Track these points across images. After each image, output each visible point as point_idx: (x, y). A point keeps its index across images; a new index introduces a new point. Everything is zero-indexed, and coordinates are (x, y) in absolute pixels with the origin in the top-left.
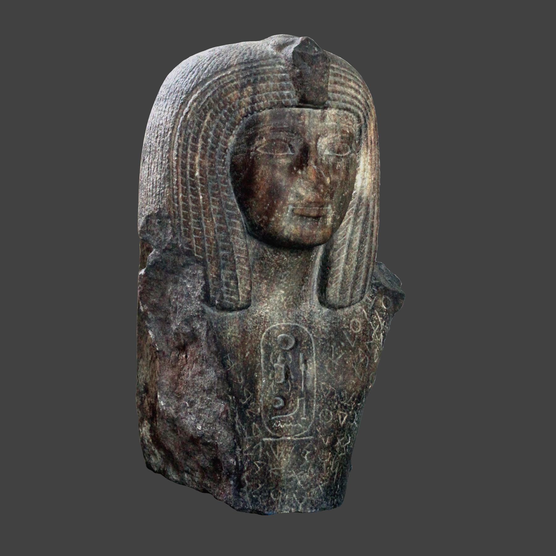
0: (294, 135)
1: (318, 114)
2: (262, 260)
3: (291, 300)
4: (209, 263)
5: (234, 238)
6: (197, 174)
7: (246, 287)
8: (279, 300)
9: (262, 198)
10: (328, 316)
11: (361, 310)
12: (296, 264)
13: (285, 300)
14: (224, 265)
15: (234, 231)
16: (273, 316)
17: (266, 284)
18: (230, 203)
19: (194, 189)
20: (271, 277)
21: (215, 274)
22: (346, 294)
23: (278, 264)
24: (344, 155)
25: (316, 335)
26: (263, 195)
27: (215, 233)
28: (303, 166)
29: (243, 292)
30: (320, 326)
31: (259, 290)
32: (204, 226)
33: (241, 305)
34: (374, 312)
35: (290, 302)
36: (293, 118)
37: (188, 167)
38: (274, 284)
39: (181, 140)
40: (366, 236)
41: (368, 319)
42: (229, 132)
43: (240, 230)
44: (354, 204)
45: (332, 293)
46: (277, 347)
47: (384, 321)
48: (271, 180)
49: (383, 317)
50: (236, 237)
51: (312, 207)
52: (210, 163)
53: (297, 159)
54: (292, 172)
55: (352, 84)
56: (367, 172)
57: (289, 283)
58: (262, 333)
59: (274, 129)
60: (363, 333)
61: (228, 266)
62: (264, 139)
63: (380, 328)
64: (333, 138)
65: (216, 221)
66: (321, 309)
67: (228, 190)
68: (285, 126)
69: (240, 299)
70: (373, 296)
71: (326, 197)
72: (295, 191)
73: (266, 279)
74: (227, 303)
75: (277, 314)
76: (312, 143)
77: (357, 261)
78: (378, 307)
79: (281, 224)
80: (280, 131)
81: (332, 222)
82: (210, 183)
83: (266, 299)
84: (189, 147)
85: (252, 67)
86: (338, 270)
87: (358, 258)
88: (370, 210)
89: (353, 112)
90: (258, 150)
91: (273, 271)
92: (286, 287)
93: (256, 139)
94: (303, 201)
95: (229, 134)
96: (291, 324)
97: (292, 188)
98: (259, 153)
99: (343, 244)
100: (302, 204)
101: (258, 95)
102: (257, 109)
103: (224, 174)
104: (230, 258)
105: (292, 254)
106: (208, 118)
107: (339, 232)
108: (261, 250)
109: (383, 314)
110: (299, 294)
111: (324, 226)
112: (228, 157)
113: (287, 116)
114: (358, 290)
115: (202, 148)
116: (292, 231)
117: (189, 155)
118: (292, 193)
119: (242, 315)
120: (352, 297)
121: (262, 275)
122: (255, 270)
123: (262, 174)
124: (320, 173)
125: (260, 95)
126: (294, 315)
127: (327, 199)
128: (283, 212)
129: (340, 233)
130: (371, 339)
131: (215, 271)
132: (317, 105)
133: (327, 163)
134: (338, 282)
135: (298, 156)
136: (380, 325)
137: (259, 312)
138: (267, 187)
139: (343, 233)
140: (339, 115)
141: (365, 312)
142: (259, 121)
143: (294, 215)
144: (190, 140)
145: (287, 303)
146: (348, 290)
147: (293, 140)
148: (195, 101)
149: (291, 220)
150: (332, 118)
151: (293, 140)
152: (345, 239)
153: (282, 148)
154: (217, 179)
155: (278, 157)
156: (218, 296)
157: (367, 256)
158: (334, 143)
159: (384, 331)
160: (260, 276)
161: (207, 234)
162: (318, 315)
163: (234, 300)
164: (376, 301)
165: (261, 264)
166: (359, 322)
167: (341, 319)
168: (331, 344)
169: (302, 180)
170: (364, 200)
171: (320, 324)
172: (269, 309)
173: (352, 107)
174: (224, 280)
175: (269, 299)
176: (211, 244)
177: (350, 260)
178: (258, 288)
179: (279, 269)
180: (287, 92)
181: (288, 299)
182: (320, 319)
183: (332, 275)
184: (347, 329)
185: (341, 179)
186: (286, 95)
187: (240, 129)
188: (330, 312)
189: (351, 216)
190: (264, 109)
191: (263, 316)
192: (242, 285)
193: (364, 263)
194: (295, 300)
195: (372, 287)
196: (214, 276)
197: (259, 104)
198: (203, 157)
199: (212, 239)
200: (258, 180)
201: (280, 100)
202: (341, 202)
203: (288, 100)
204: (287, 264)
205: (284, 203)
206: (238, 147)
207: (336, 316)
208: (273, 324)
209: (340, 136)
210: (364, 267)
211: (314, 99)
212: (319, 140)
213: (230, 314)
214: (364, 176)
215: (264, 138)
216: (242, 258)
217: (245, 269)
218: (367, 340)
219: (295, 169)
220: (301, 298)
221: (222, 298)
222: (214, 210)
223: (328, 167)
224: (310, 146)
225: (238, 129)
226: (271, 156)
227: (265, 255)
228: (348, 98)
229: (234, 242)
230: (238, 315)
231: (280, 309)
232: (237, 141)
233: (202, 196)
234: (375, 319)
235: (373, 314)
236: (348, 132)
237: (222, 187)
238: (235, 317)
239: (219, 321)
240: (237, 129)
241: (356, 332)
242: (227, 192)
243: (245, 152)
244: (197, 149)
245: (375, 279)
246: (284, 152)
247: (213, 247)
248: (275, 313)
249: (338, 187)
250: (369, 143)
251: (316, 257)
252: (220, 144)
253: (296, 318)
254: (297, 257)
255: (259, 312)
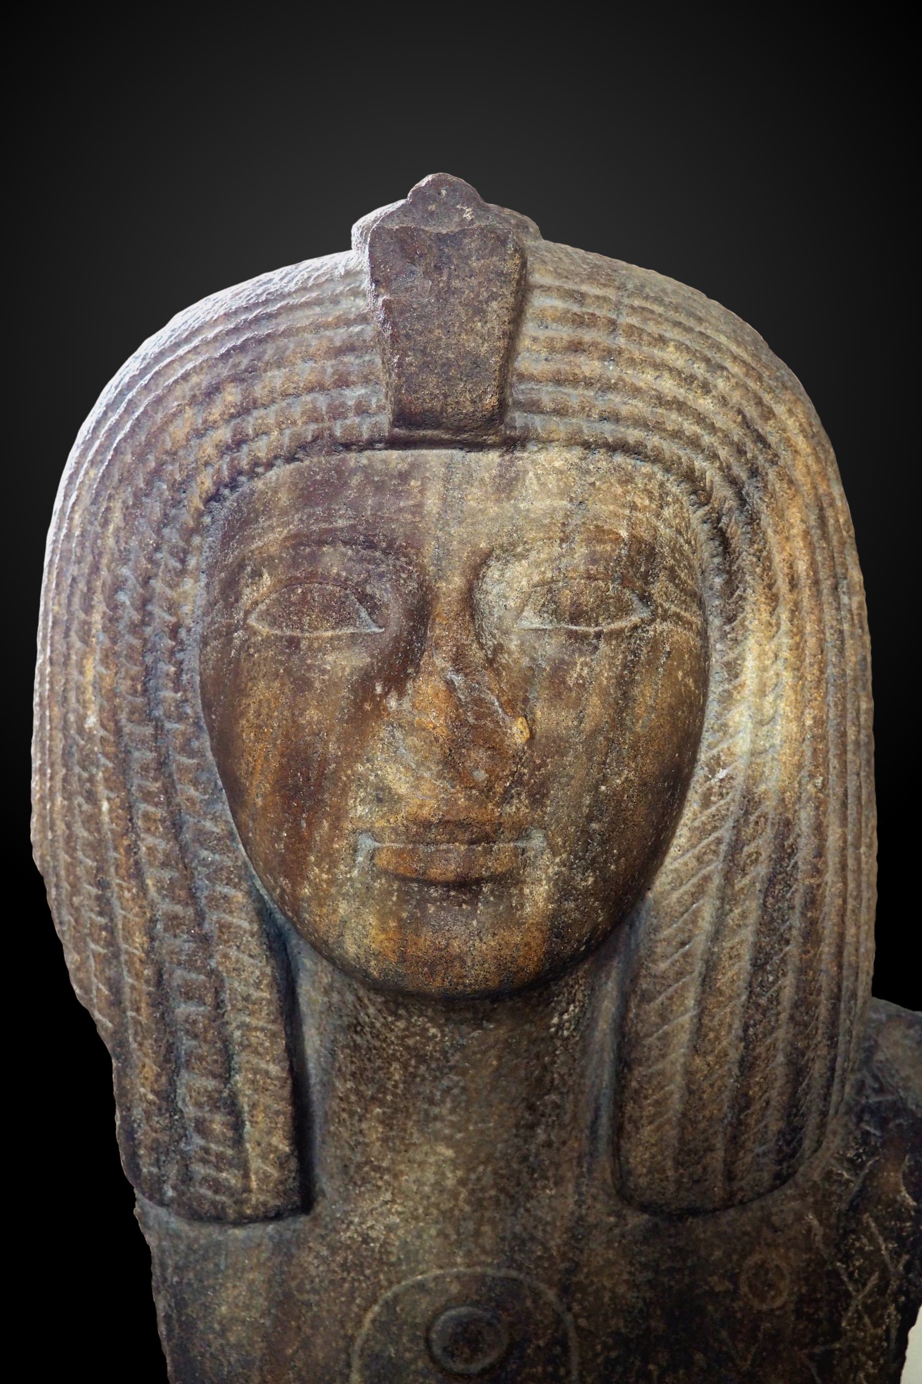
0: (378, 554)
1: (488, 468)
2: (356, 1032)
3: (488, 1180)
4: (134, 1046)
5: (226, 956)
6: (92, 721)
7: (275, 1141)
8: (437, 1183)
9: (264, 808)
10: (645, 1241)
11: (799, 1218)
12: (484, 1053)
13: (462, 1182)
14: (189, 1054)
15: (223, 927)
16: (418, 1243)
17: (382, 1122)
18: (208, 825)
19: (85, 775)
20: (395, 1095)
21: (153, 1091)
22: (705, 1169)
23: (407, 1048)
24: (606, 628)
25: (587, 1318)
26: (264, 796)
27: (152, 939)
28: (408, 676)
29: (264, 1157)
30: (608, 1284)
31: (358, 1143)
32: (120, 912)
33: (255, 1208)
34: (859, 1222)
35: (483, 1190)
36: (380, 488)
37: (72, 699)
38: (410, 1124)
39: (60, 605)
40: (788, 942)
41: (825, 1253)
42: (178, 565)
43: (246, 925)
44: (724, 818)
45: (642, 1162)
46: (420, 1364)
47: (906, 1257)
48: (287, 736)
49: (900, 1240)
50: (233, 953)
51: (435, 842)
52: (129, 683)
53: (393, 652)
54: (364, 700)
55: (670, 355)
56: (779, 697)
57: (468, 1120)
58: (366, 1310)
59: (295, 536)
60: (799, 1314)
61: (201, 1058)
62: (267, 579)
63: (887, 1284)
64: (551, 560)
65: (159, 890)
66: (619, 1215)
67: (204, 778)
68: (341, 523)
69: (254, 1185)
70: (859, 1155)
71: (506, 798)
72: (372, 778)
73: (382, 1103)
74: (203, 1197)
75: (433, 1232)
76: (448, 582)
77: (745, 1038)
78: (879, 1201)
79: (335, 911)
80: (321, 543)
81: (549, 899)
82: (136, 754)
83: (386, 1177)
84: (75, 626)
85: (257, 320)
86: (661, 1073)
87: (746, 1028)
88: (802, 841)
89: (656, 458)
90: (252, 621)
91: (397, 1077)
92: (459, 1136)
93: (243, 582)
94: (399, 819)
95: (175, 569)
96: (490, 1271)
97: (360, 768)
98: (255, 633)
99: (680, 974)
100: (394, 830)
101: (255, 413)
102: (244, 464)
103: (181, 718)
104: (206, 1031)
105: (454, 1016)
106: (117, 517)
107: (656, 929)
108: (350, 998)
109: (902, 1229)
110: (525, 1158)
111: (510, 918)
112: (191, 658)
113: (355, 481)
114: (759, 1150)
115: (105, 629)
116: (366, 941)
117: (74, 657)
118: (360, 786)
119: (288, 1235)
120: (730, 1176)
121: (362, 1088)
122: (340, 1070)
123: (258, 714)
124: (479, 702)
125: (262, 412)
126: (508, 1235)
127: (517, 808)
128: (334, 864)
129: (666, 933)
130: (837, 1333)
131: (152, 1079)
132: (459, 430)
133: (525, 662)
134: (669, 1121)
135: (397, 640)
136: (884, 1270)
137: (361, 1223)
138: (274, 764)
139: (681, 930)
140: (588, 472)
141: (815, 1223)
142: (256, 511)
143: (378, 877)
144: (76, 600)
145: (471, 1193)
146: (711, 1149)
147: (381, 575)
148: (92, 463)
149: (365, 895)
150: (552, 482)
151: (381, 575)
152: (686, 955)
153: (326, 609)
154: (155, 737)
155: (316, 645)
156: (173, 1171)
157: (792, 1018)
158: (553, 581)
159: (907, 1294)
160: (357, 1092)
161: (126, 939)
162: (604, 1238)
163: (229, 1188)
164: (871, 1175)
165: (356, 1047)
166: (783, 1265)
167: (703, 1253)
168: (645, 1361)
169: (398, 734)
170: (769, 806)
171: (611, 1276)
172: (399, 1213)
173: (654, 441)
174: (191, 1111)
175: (396, 1176)
176: (138, 976)
177: (712, 1035)
178: (355, 1134)
179: (416, 1067)
180: (360, 391)
181: (473, 1176)
182: (611, 1254)
183: (636, 1092)
184: (727, 1292)
185: (587, 726)
186: (351, 403)
187: (210, 548)
188: (656, 1225)
189: (711, 868)
190: (270, 465)
191: (373, 1240)
192: (261, 1131)
193: (780, 1045)
194: (503, 1183)
195: (860, 1119)
196: (151, 1097)
197: (254, 445)
198: (107, 658)
199: (141, 961)
200: (248, 736)
201: (327, 424)
202: (590, 818)
203: (357, 420)
204: (444, 1053)
205: (335, 826)
206: (209, 619)
207: (681, 1244)
208: (413, 1272)
209: (584, 550)
210: (781, 1058)
211: (437, 405)
212: (493, 572)
213: (239, 1233)
214: (759, 709)
215: (266, 575)
216: (256, 1029)
217: (267, 1073)
218: (814, 1342)
219: (379, 690)
220: (533, 1171)
221: (187, 1178)
222: (151, 850)
223: (529, 677)
224: (437, 597)
225: (206, 548)
226: (293, 643)
227: (363, 1017)
228: (639, 407)
229: (228, 972)
230: (271, 1238)
231: (443, 1213)
232: (208, 593)
233: (109, 799)
234: (861, 1250)
235: (853, 1231)
236: (624, 534)
237: (182, 769)
238: (259, 1245)
239: (192, 1258)
240: (200, 549)
241: (765, 1307)
242: (195, 783)
243: (221, 636)
244: (90, 630)
245: (881, 1090)
246: (340, 623)
247: (145, 987)
248: (422, 1230)
249: (570, 758)
250: (782, 585)
251: (584, 1023)
252: (153, 608)
253: (512, 1249)
254: (480, 1026)
255: (361, 1223)
